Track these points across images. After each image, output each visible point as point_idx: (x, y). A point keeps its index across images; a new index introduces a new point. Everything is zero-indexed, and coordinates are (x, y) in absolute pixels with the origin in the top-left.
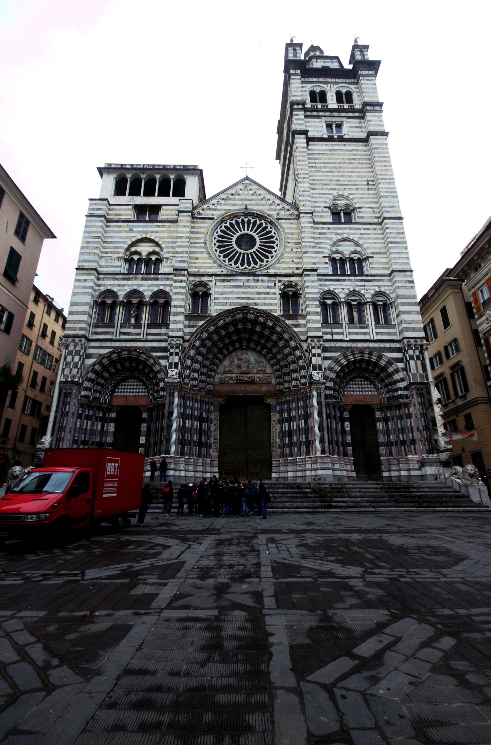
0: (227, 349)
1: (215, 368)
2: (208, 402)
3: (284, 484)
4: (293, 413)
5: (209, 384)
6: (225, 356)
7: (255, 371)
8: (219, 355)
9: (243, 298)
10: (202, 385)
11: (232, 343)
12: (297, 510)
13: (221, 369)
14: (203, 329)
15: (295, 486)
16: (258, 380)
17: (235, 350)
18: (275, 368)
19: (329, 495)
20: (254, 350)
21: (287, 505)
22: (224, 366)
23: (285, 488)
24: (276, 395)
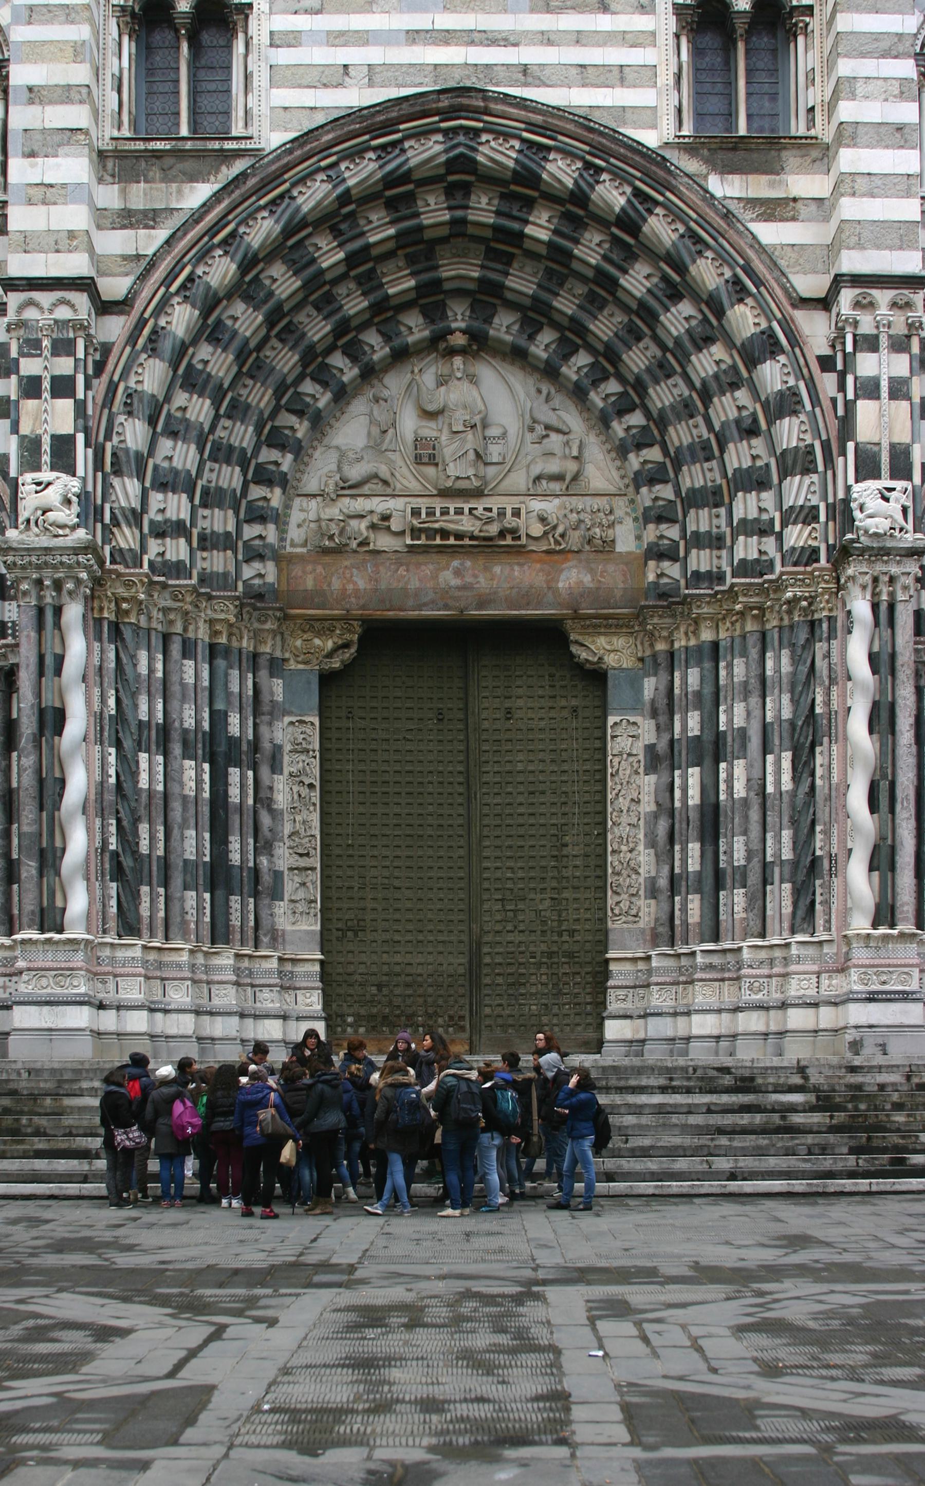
0: (353, 352)
1: (287, 462)
2: (255, 656)
3: (668, 1072)
4: (735, 715)
5: (254, 555)
6: (342, 395)
7: (519, 480)
8: (308, 387)
9: (446, 37)
10: (218, 561)
11: (384, 312)
12: (734, 1186)
13: (320, 471)
14: (215, 231)
15: (727, 1080)
16: (537, 530)
17: (401, 355)
18: (634, 461)
19: (900, 1118)
20: (517, 355)
21: (682, 1164)
22: (342, 455)
23: (675, 1090)
24: (640, 615)
